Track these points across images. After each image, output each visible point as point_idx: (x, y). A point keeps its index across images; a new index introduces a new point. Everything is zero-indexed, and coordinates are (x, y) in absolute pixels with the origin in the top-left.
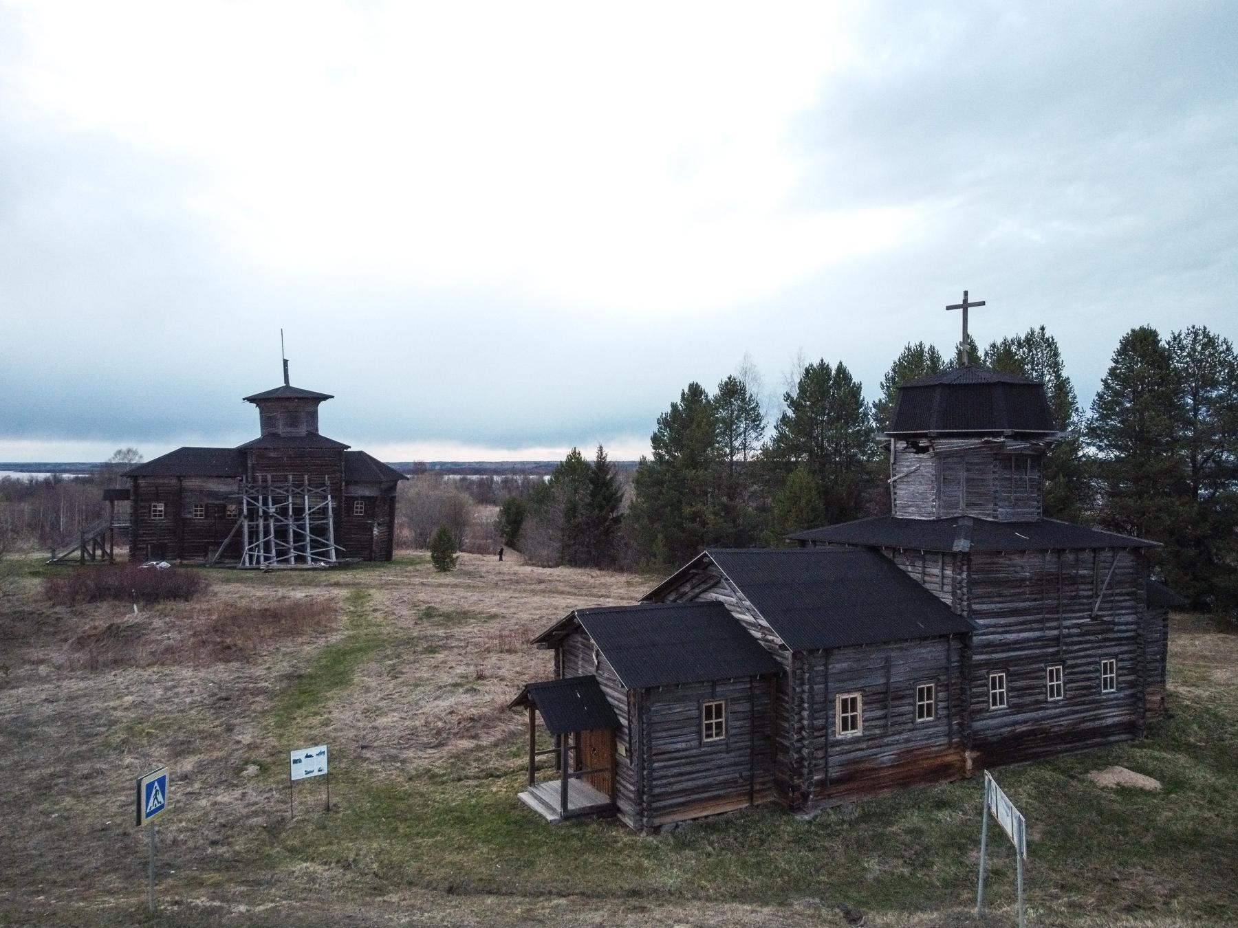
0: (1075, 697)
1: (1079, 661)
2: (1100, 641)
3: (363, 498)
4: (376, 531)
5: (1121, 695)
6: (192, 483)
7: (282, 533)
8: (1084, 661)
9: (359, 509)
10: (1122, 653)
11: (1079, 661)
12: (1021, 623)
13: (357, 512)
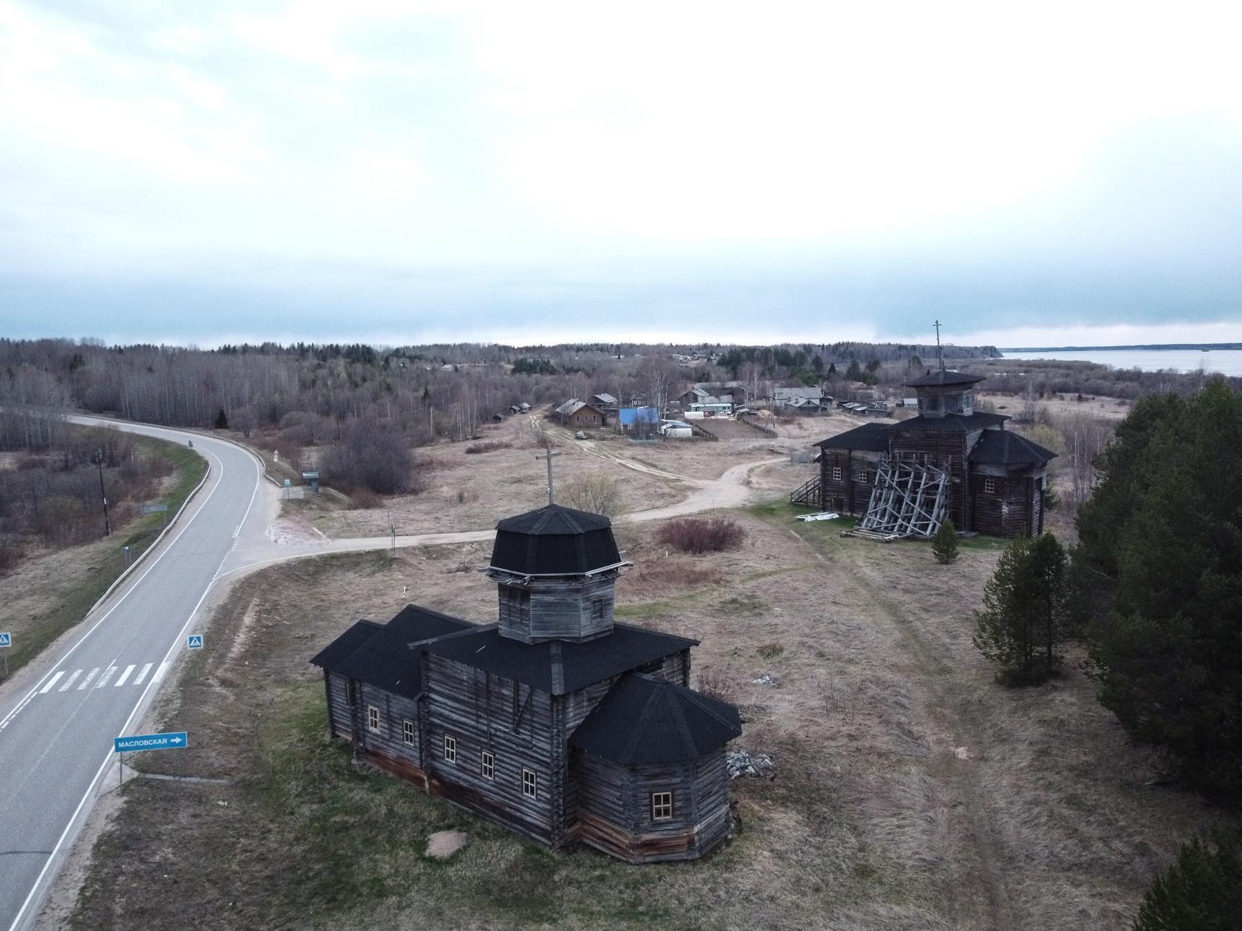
0: (502, 784)
1: (505, 759)
2: (521, 752)
3: (991, 477)
4: (1005, 509)
5: (540, 805)
6: (858, 454)
7: (899, 501)
8: (508, 761)
9: (989, 490)
10: (540, 772)
11: (505, 759)
12: (464, 711)
13: (988, 490)
